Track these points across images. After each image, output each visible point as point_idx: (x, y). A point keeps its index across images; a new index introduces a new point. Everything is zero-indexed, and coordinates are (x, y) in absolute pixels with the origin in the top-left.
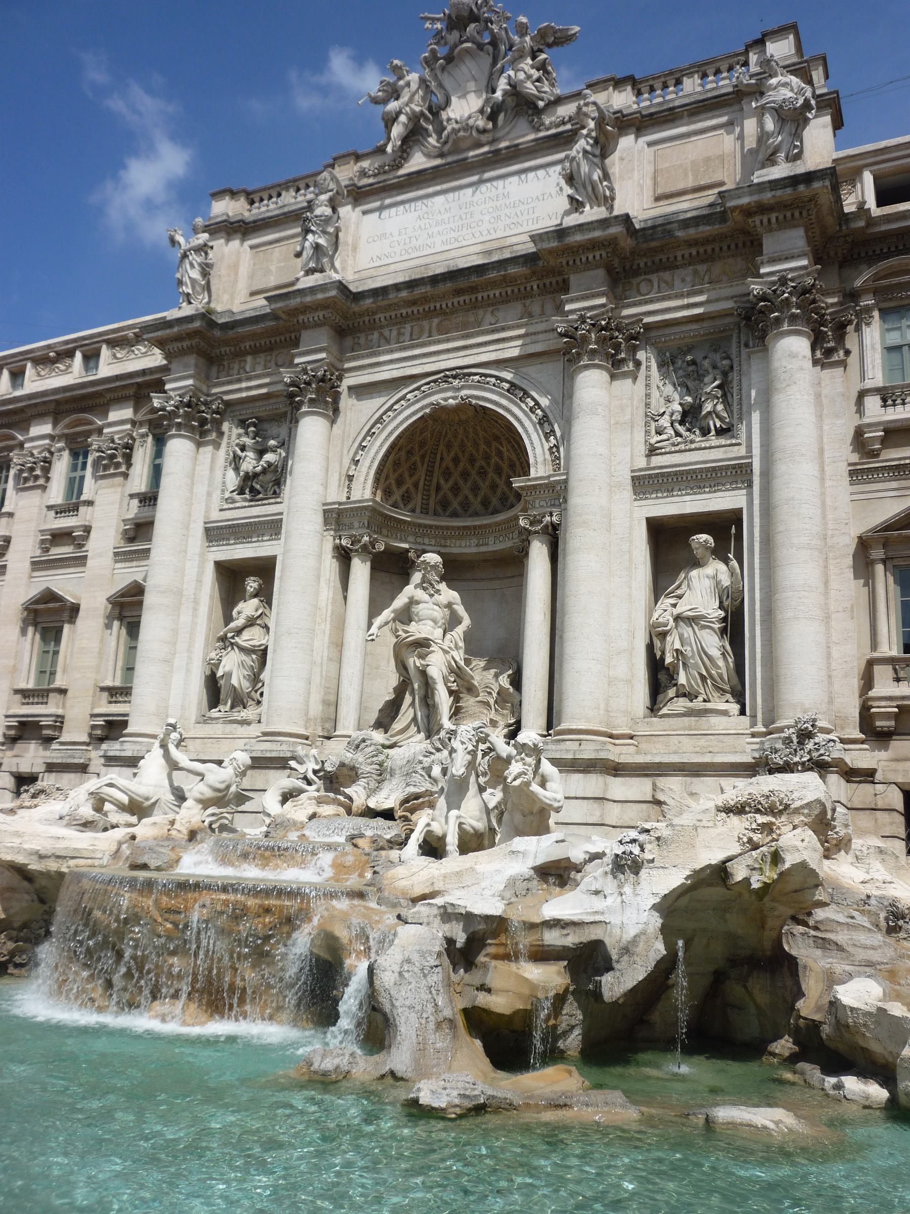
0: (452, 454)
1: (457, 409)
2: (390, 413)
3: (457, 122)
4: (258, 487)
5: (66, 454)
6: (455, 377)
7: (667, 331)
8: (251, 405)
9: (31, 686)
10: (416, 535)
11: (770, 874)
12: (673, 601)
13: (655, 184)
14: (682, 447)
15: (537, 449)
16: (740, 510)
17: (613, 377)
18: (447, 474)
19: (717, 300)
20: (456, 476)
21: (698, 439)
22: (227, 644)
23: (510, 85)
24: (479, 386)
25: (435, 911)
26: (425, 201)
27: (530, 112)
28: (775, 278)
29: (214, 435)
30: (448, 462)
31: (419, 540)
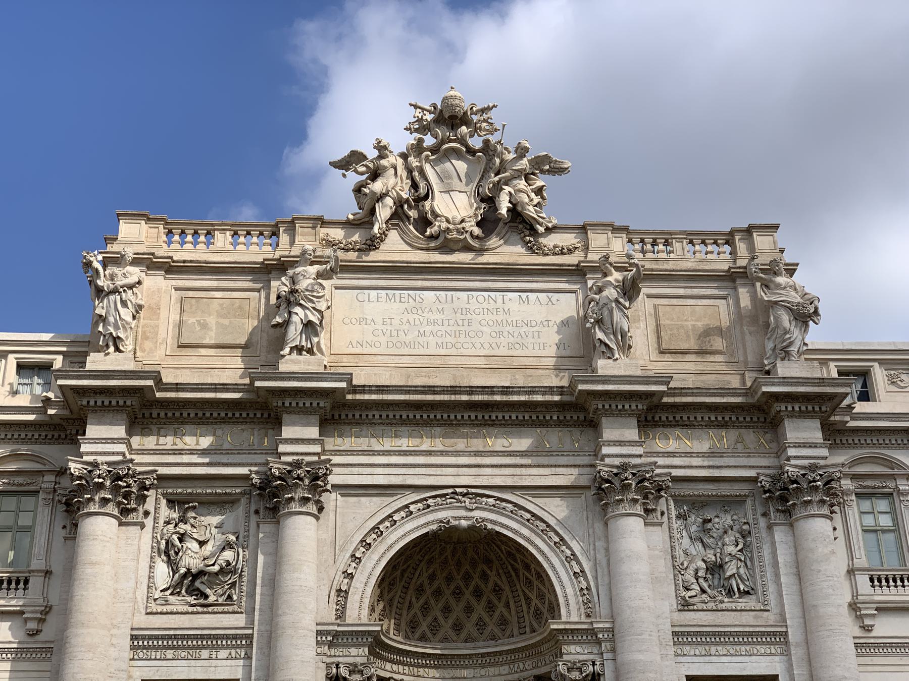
0: (431, 571)
2: (387, 524)
3: (448, 221)
6: (464, 495)
7: (685, 485)
10: (392, 662)
13: (659, 337)
14: (711, 605)
15: (566, 589)
18: (420, 590)
20: (429, 591)
21: (726, 600)
23: (510, 202)
24: (493, 509)
26: (411, 292)
27: (527, 232)
28: (806, 462)
29: (138, 516)
30: (424, 578)
31: (395, 667)
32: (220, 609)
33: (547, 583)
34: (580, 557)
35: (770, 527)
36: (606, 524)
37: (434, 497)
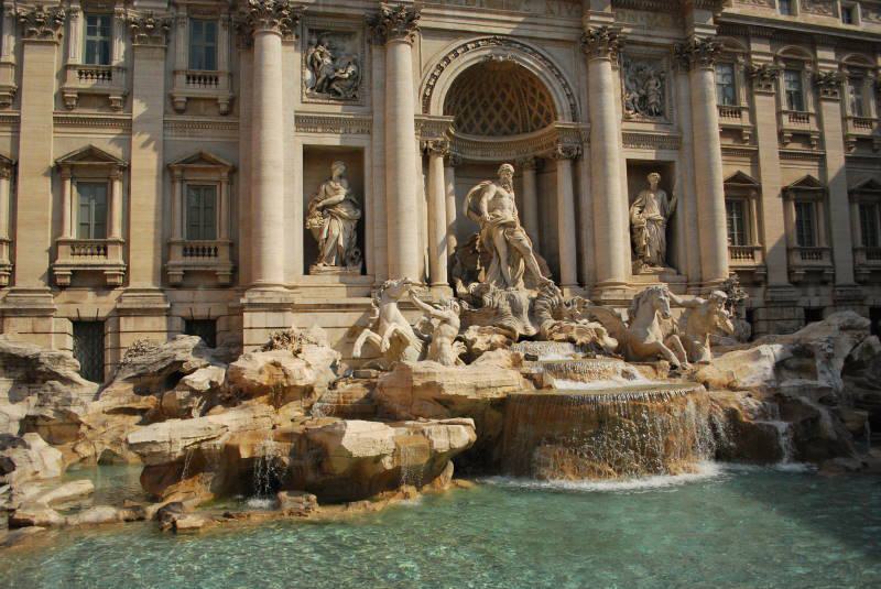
1: (505, 63)
4: (337, 88)
5: (80, 15)
8: (323, 19)
9: (74, 237)
11: (869, 356)
12: (638, 209)
15: (561, 103)
16: (673, 162)
17: (614, 69)
18: (464, 103)
19: (662, 37)
20: (468, 105)
22: (325, 212)
25: (796, 389)
28: (705, 37)
32: (349, 103)
33: (547, 100)
34: (570, 84)
35: (675, 75)
36: (587, 67)
37: (482, 40)
